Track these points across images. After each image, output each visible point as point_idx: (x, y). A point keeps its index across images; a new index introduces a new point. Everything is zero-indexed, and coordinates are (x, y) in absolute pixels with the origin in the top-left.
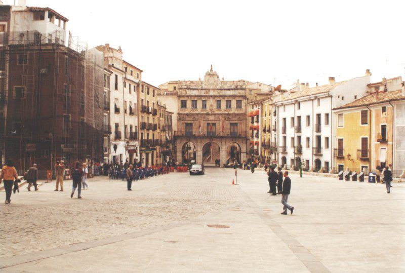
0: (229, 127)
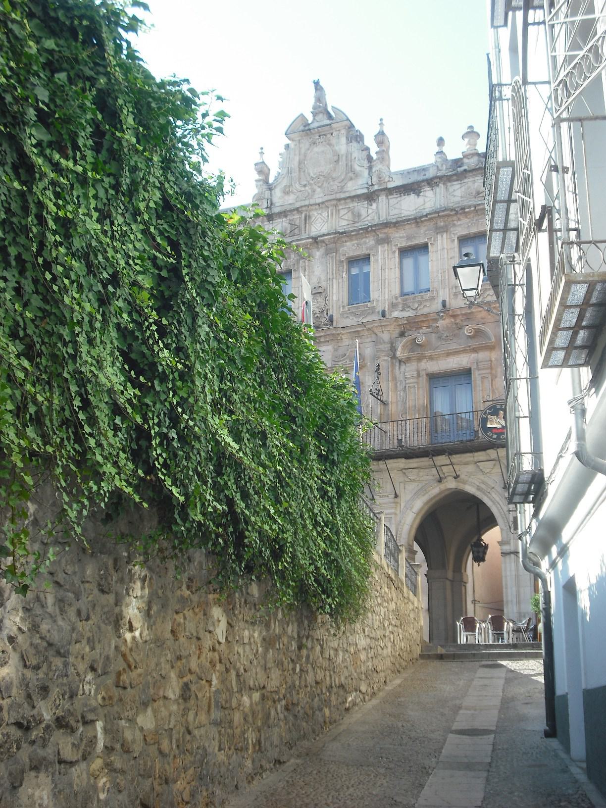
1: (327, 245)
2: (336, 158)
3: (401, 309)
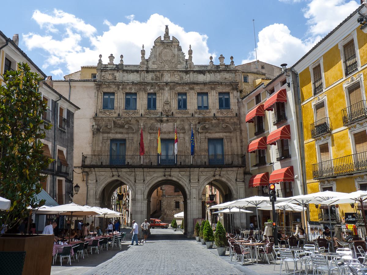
0: (205, 145)
1: (170, 86)
2: (173, 55)
3: (198, 114)
